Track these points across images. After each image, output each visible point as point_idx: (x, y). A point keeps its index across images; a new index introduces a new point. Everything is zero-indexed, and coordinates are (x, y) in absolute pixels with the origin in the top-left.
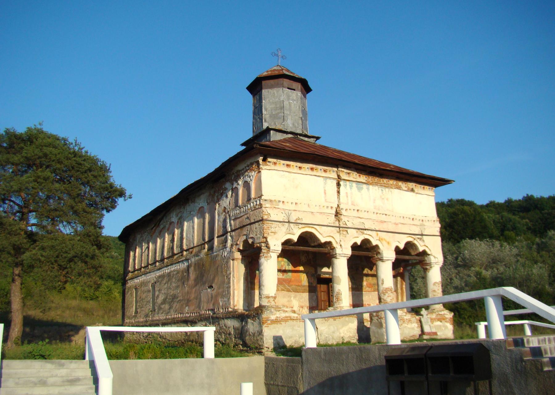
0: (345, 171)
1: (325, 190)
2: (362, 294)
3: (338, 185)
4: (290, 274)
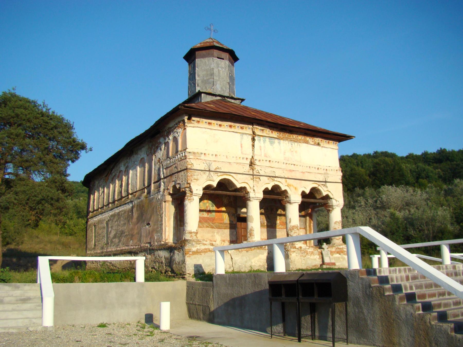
0: (259, 128)
1: (241, 144)
2: (276, 230)
3: (253, 139)
4: (214, 214)
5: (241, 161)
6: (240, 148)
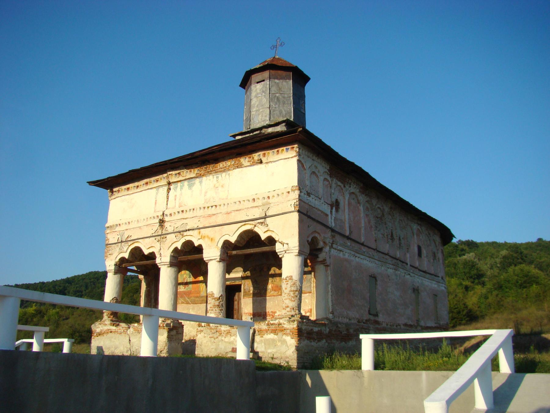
2: (266, 300)
3: (169, 189)
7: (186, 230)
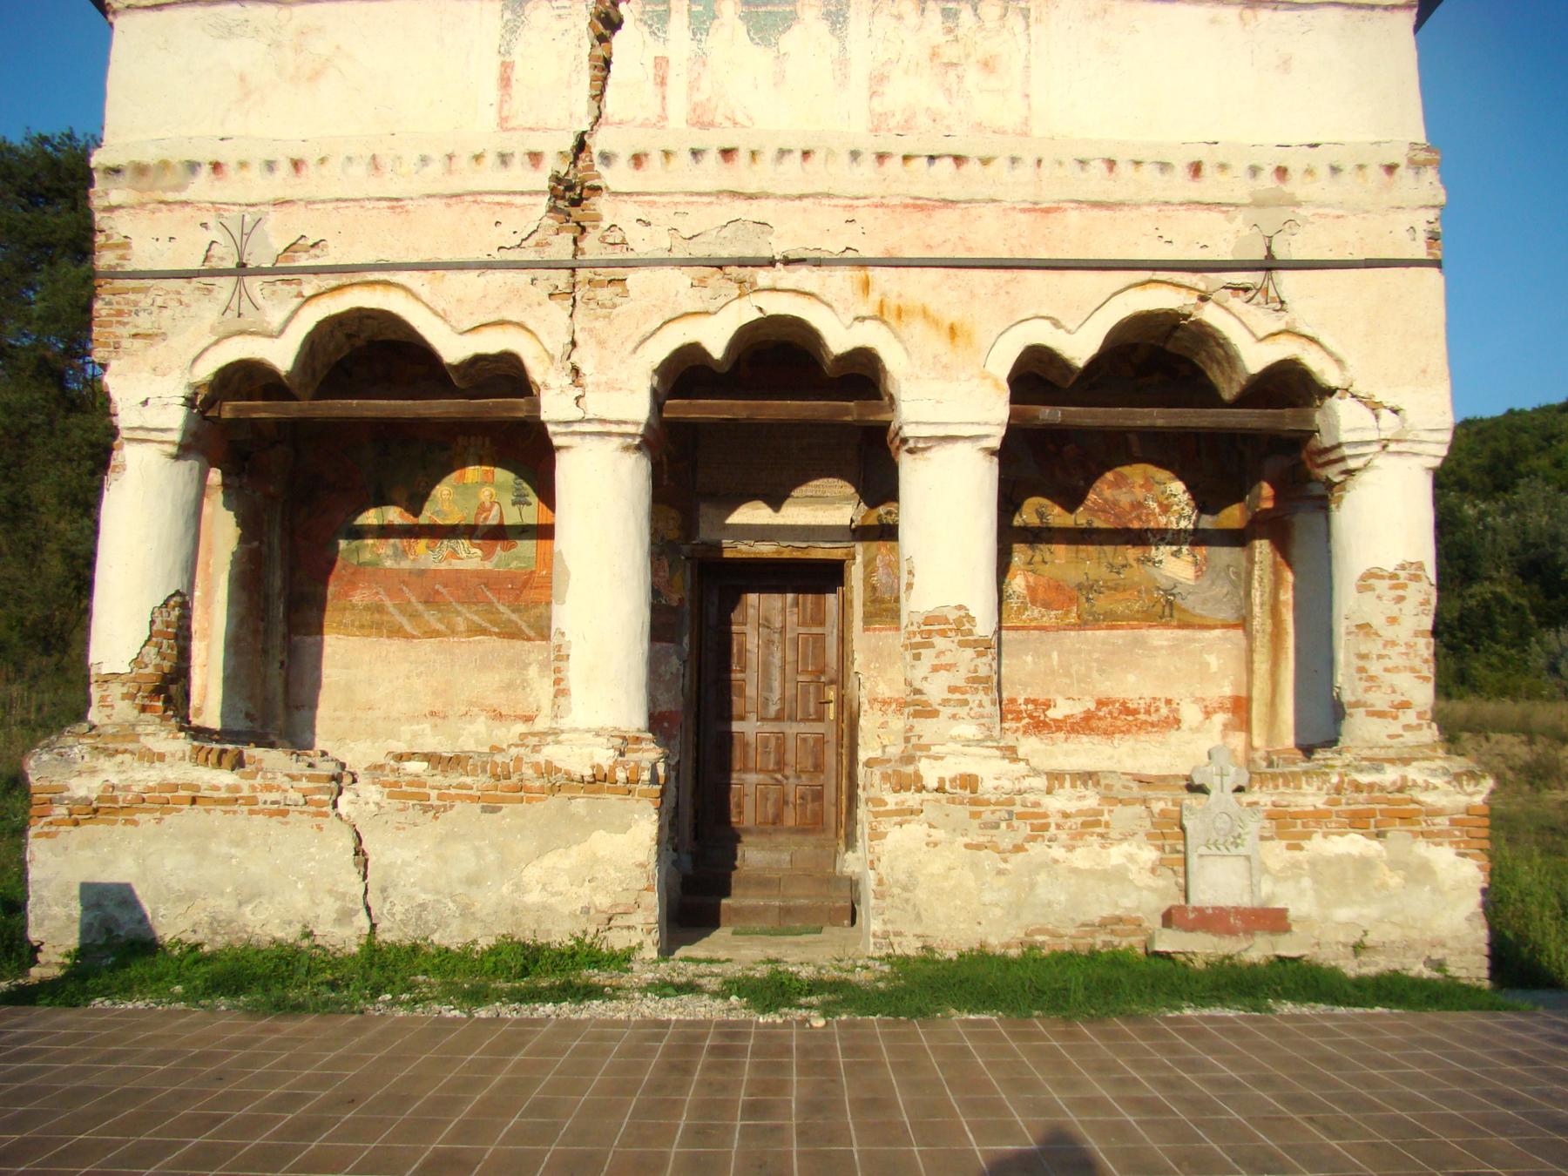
1: (507, 67)
5: (491, 178)
6: (492, 92)
7: (772, 263)
